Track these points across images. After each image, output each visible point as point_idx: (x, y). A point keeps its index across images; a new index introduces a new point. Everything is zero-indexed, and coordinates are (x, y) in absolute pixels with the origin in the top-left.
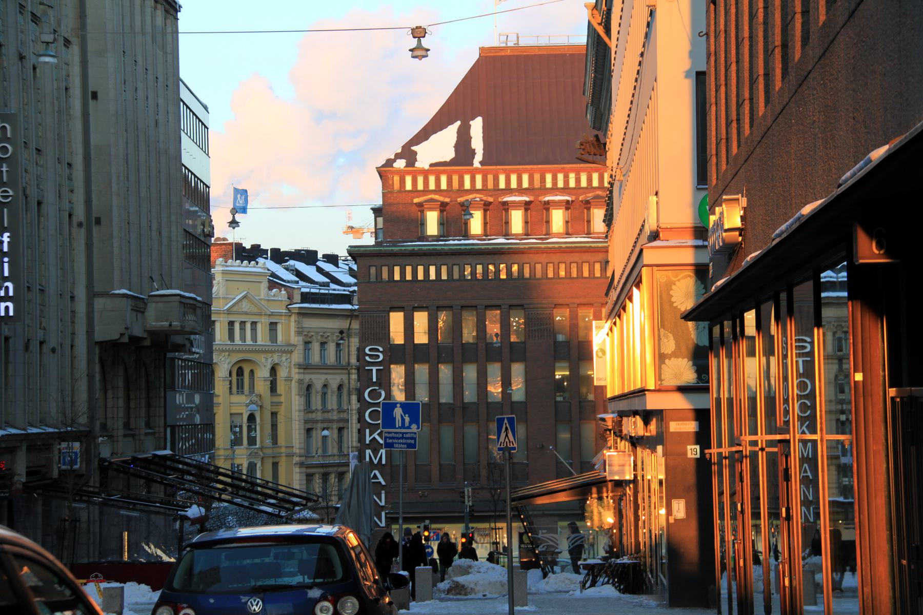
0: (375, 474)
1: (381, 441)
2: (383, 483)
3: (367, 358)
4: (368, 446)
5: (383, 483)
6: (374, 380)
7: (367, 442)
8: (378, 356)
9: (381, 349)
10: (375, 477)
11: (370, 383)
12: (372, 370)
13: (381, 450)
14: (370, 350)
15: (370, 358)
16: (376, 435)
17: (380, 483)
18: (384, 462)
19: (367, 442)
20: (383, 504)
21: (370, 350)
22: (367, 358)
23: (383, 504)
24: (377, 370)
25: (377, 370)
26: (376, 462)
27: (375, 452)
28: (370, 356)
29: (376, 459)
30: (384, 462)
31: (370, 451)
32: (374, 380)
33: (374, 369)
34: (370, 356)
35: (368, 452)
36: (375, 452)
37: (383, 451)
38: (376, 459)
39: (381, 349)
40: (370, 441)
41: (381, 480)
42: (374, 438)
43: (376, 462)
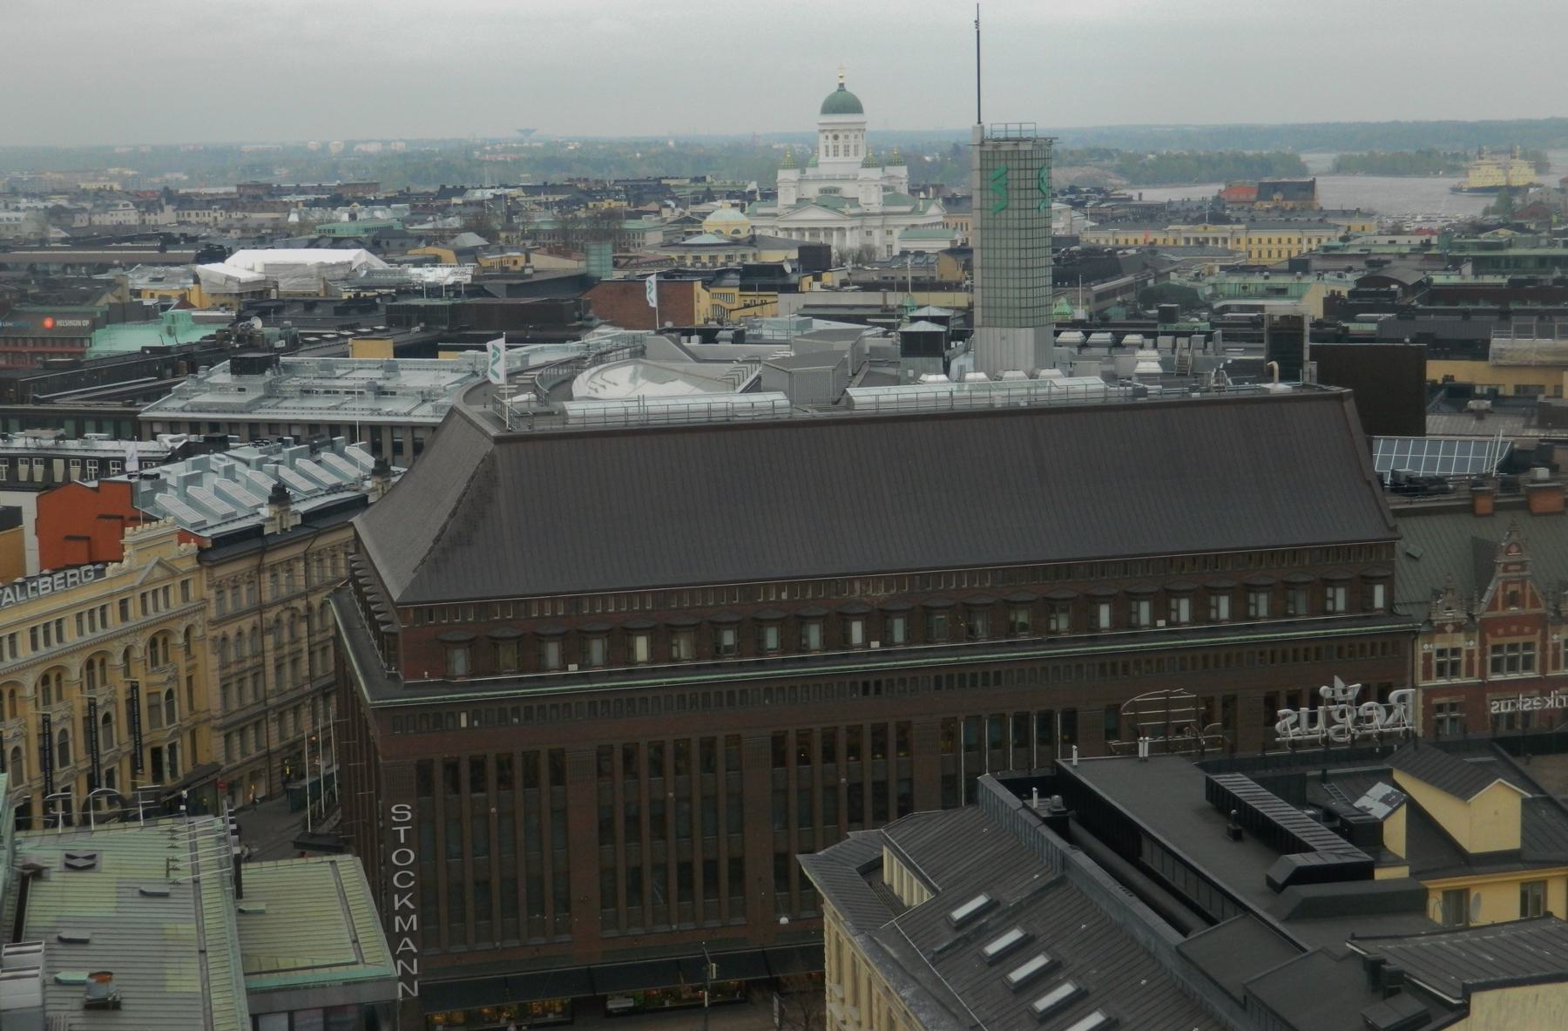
6: (402, 840)
14: (397, 809)
16: (405, 900)
17: (411, 951)
20: (415, 972)
23: (415, 972)
26: (406, 929)
27: (406, 918)
28: (397, 815)
32: (402, 840)
33: (402, 829)
34: (397, 815)
36: (406, 918)
41: (413, 947)
43: (406, 929)
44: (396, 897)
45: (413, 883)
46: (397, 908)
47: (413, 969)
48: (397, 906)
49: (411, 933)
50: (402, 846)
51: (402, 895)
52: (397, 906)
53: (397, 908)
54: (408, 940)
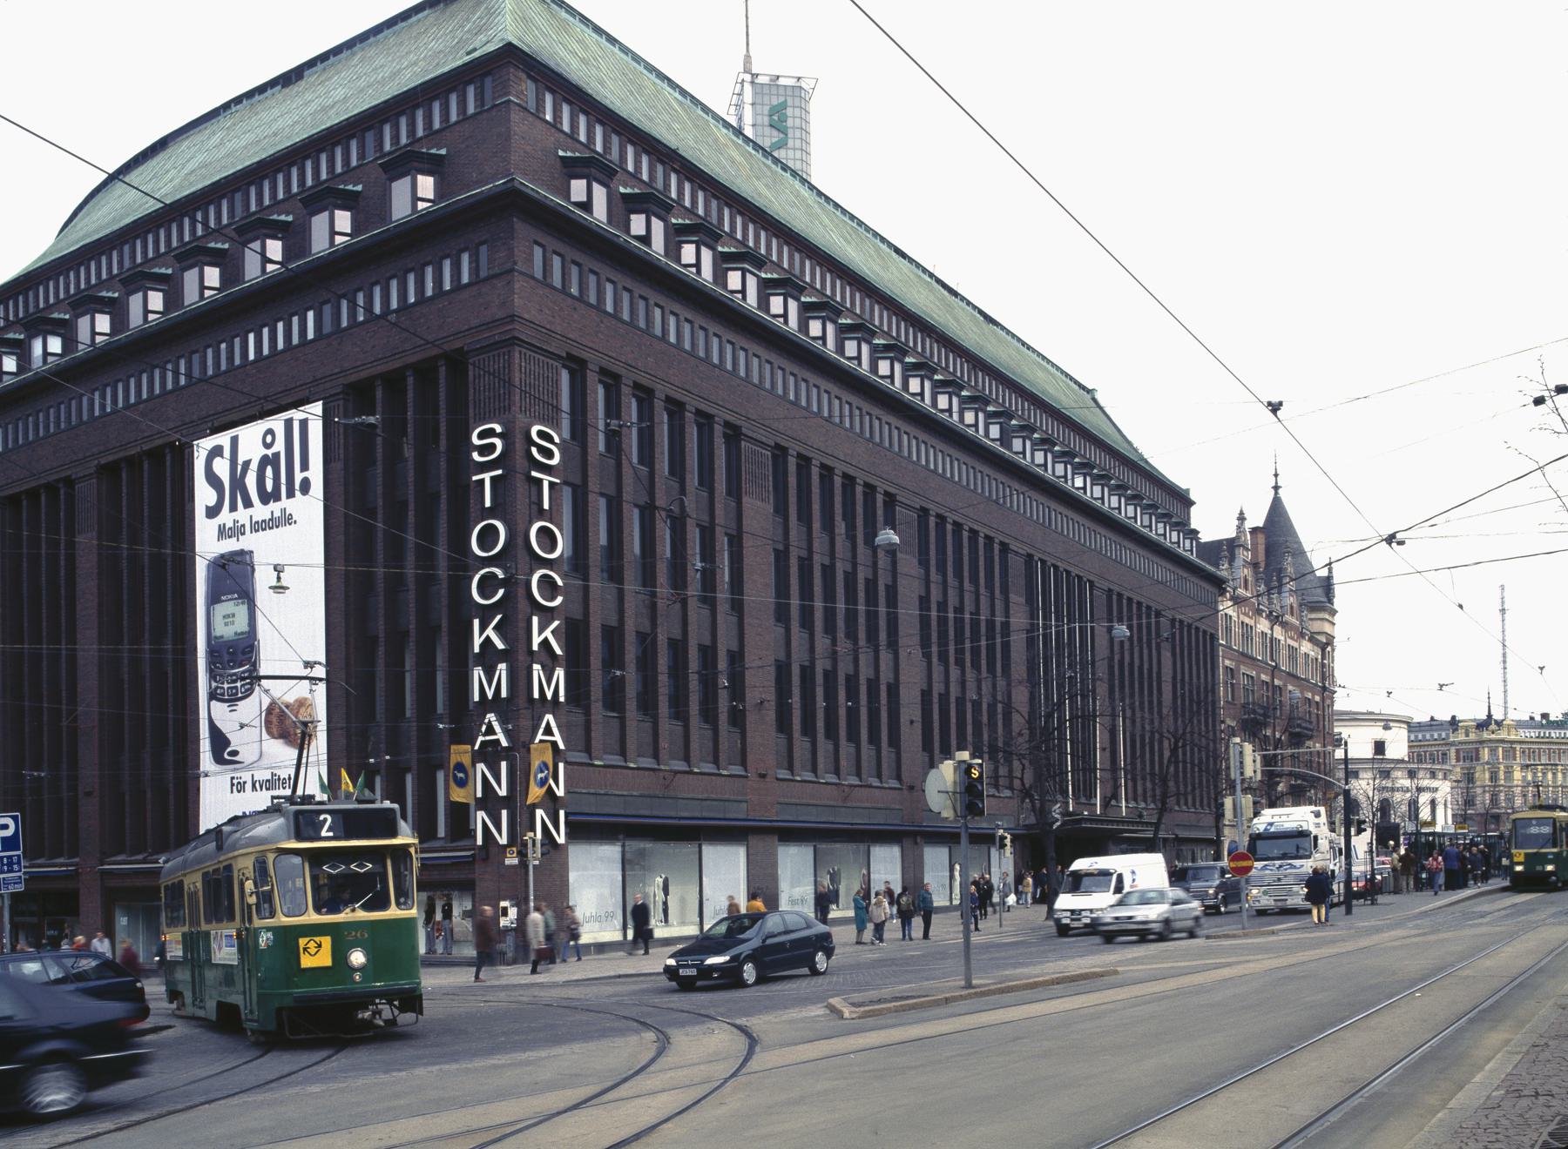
1: (500, 645)
2: (504, 743)
3: (476, 456)
5: (504, 743)
6: (488, 504)
8: (492, 447)
9: (498, 429)
10: (490, 730)
14: (481, 436)
15: (481, 454)
16: (490, 632)
17: (498, 741)
18: (504, 694)
19: (477, 650)
20: (503, 792)
21: (481, 436)
24: (492, 478)
25: (492, 478)
26: (490, 694)
27: (490, 673)
30: (504, 694)
32: (488, 504)
33: (487, 477)
36: (490, 673)
37: (502, 666)
40: (482, 646)
42: (488, 637)
43: (490, 694)
44: (535, 620)
45: (501, 592)
46: (535, 648)
51: (485, 614)
53: (535, 648)
54: (491, 717)
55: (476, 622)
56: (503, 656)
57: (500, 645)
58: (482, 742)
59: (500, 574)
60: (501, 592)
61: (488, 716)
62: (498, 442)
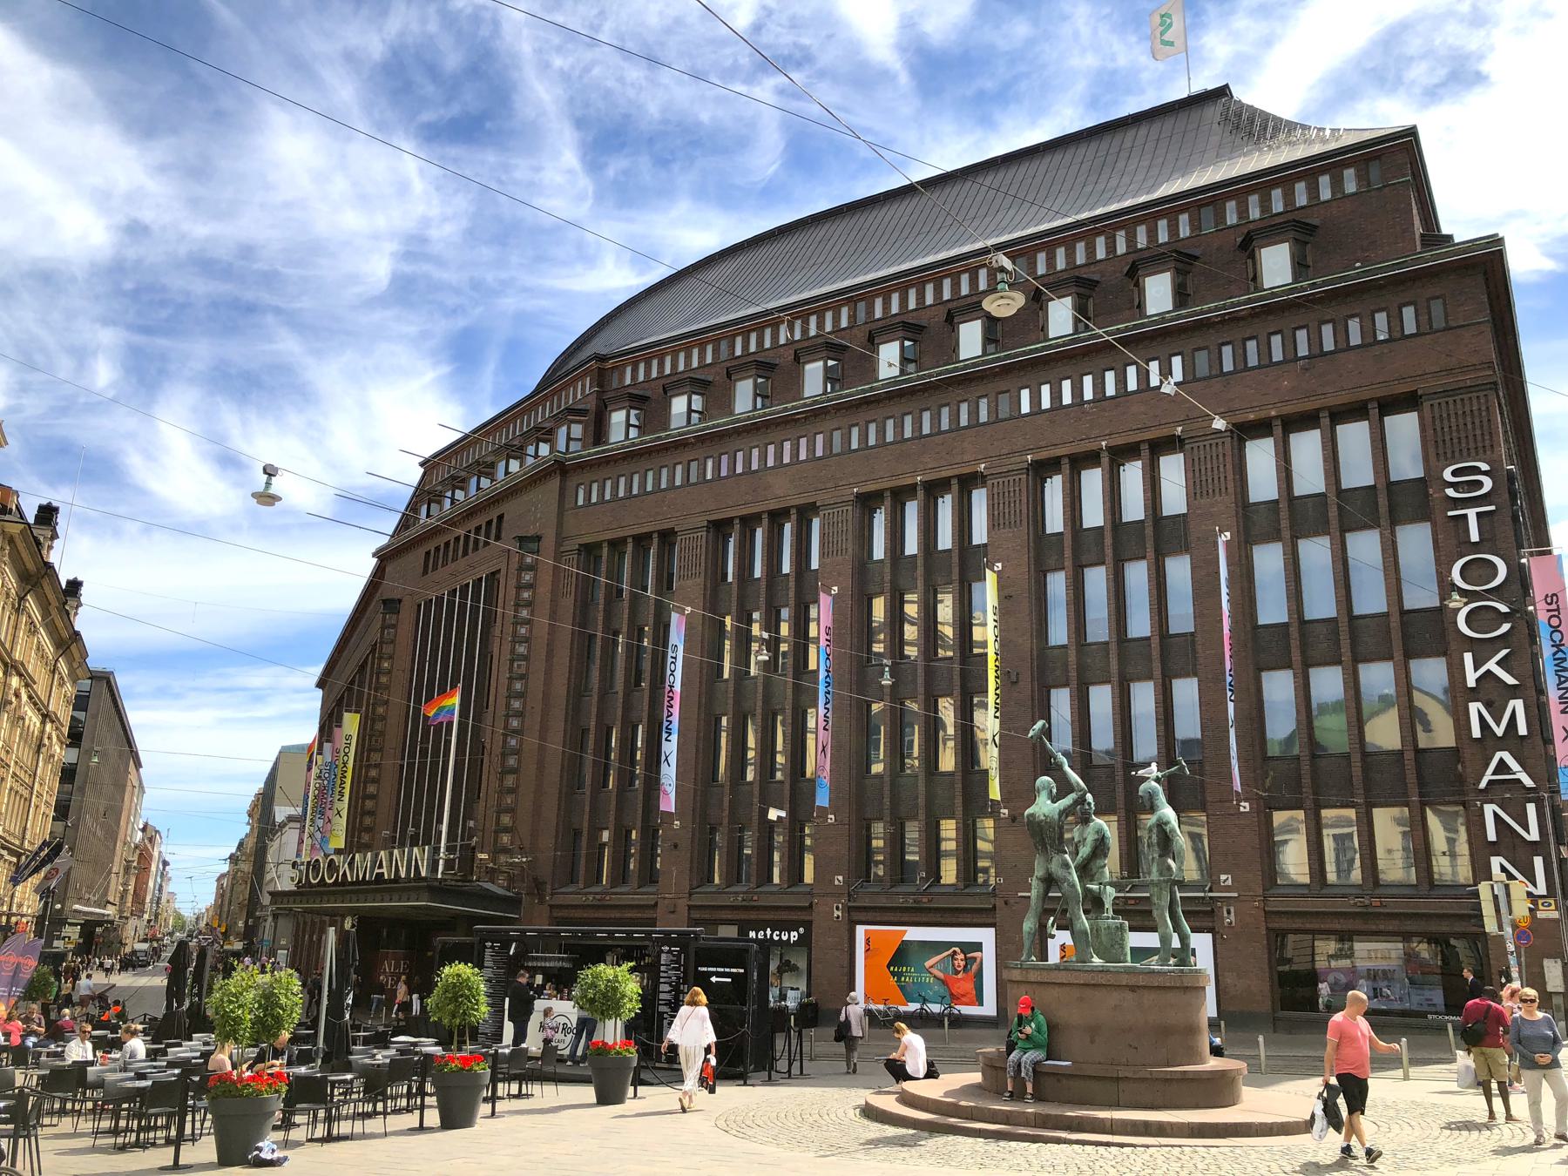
0: (1501, 760)
2: (1528, 781)
3: (1450, 492)
4: (1474, 694)
5: (1528, 781)
6: (1475, 536)
7: (1471, 683)
8: (1480, 484)
9: (1484, 467)
10: (1502, 767)
11: (1466, 546)
12: (1465, 516)
13: (1512, 703)
14: (1454, 473)
16: (1491, 665)
17: (1518, 781)
18: (1522, 730)
19: (1471, 683)
20: (1534, 835)
21: (1454, 473)
22: (1450, 492)
23: (1534, 835)
26: (1499, 731)
29: (1498, 726)
30: (1522, 730)
31: (1479, 705)
32: (1475, 536)
33: (1472, 513)
35: (1475, 708)
37: (1517, 705)
38: (1498, 726)
39: (1484, 467)
40: (1477, 680)
43: (1499, 731)
47: (1527, 829)
48: (1471, 679)
49: (1511, 739)
50: (1485, 544)
52: (1471, 679)
54: (1507, 757)
55: (1468, 658)
56: (1513, 692)
57: (1510, 680)
58: (1490, 782)
59: (1504, 608)
60: (1506, 627)
61: (1498, 755)
62: (1447, 475)
